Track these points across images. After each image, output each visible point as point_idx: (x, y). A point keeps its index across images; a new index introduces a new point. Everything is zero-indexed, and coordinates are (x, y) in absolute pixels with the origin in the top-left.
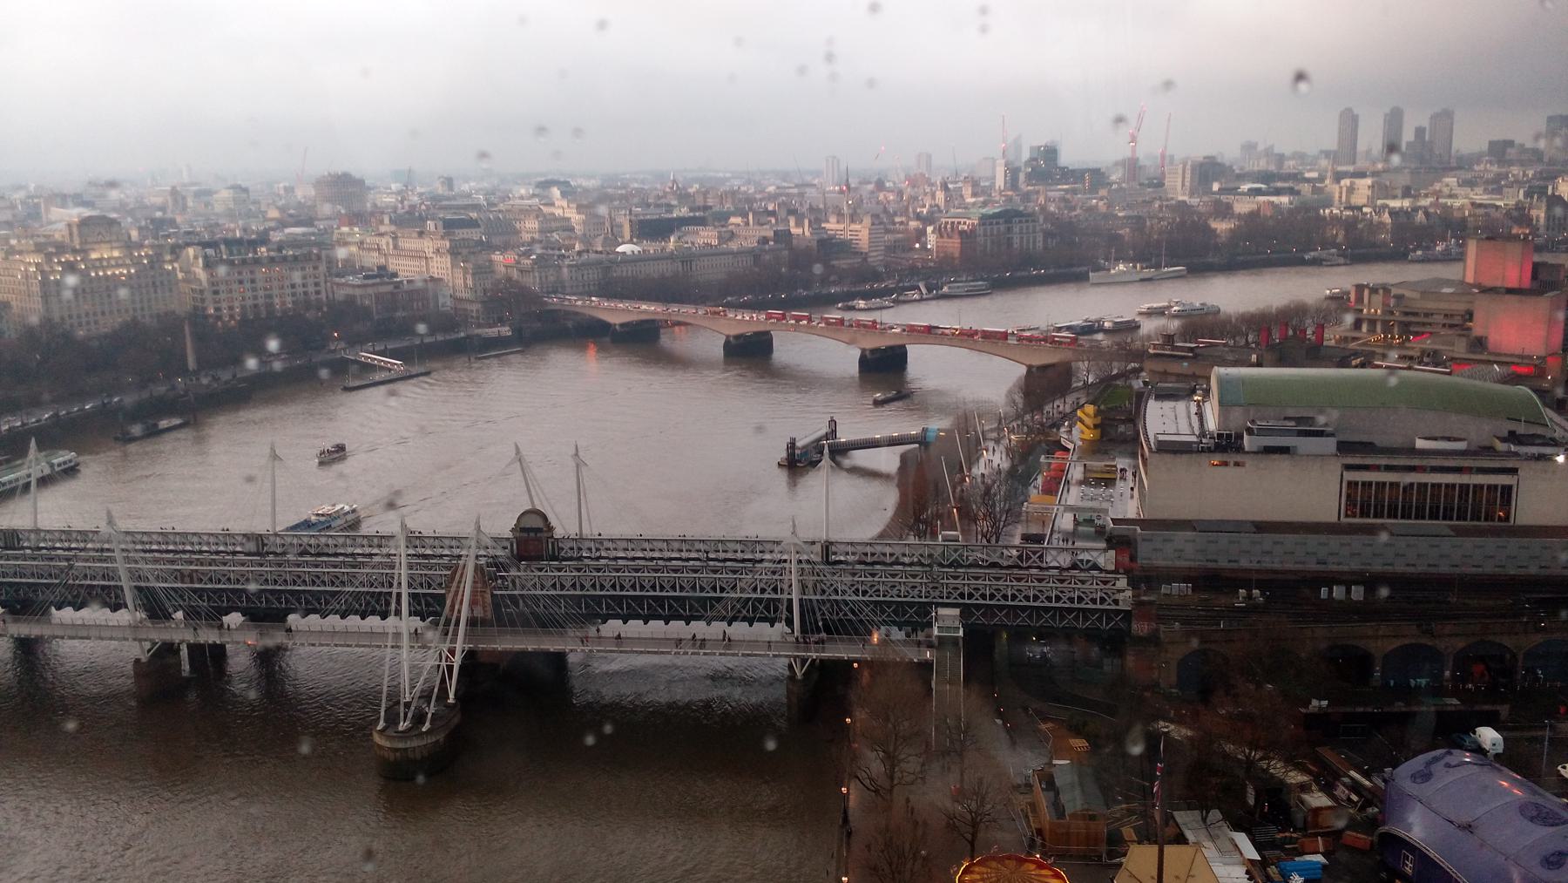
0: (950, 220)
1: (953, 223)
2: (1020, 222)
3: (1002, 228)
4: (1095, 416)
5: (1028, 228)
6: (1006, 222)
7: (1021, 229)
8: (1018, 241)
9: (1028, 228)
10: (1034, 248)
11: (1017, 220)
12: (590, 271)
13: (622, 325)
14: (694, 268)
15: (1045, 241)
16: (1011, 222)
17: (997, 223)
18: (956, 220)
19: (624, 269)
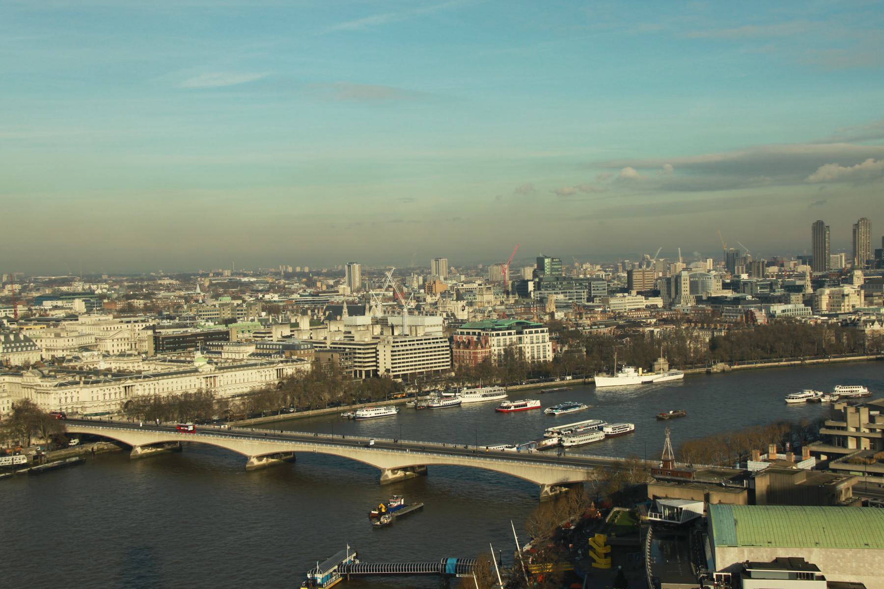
0: (465, 331)
1: (468, 333)
2: (531, 333)
4: (605, 545)
5: (538, 338)
6: (518, 333)
7: (532, 339)
8: (529, 350)
9: (538, 338)
10: (545, 357)
11: (528, 330)
12: (113, 391)
14: (218, 384)
16: (521, 333)
17: (510, 334)
19: (147, 387)
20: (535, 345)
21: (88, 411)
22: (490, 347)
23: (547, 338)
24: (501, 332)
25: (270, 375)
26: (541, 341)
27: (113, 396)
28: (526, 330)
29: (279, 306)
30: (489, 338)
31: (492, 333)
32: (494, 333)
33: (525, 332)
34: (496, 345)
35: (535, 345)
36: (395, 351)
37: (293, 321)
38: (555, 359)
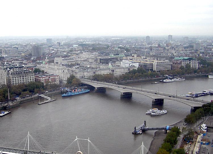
1: (176, 60)
3: (188, 62)
13: (97, 88)
14: (114, 72)
15: (199, 65)
18: (177, 60)
20: (194, 64)
21: (86, 77)
23: (197, 63)
27: (91, 74)
29: (129, 49)
35: (194, 64)
37: (133, 55)
38: (199, 68)
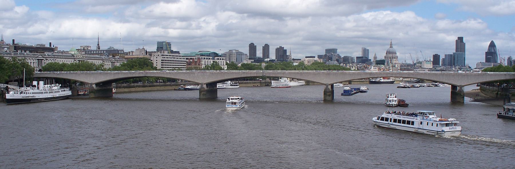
11: (217, 58)
22: (201, 65)
24: (206, 57)
25: (109, 65)
26: (222, 65)
28: (216, 57)
30: (201, 60)
31: (202, 57)
32: (203, 57)
33: (215, 59)
34: (204, 64)
36: (164, 60)
